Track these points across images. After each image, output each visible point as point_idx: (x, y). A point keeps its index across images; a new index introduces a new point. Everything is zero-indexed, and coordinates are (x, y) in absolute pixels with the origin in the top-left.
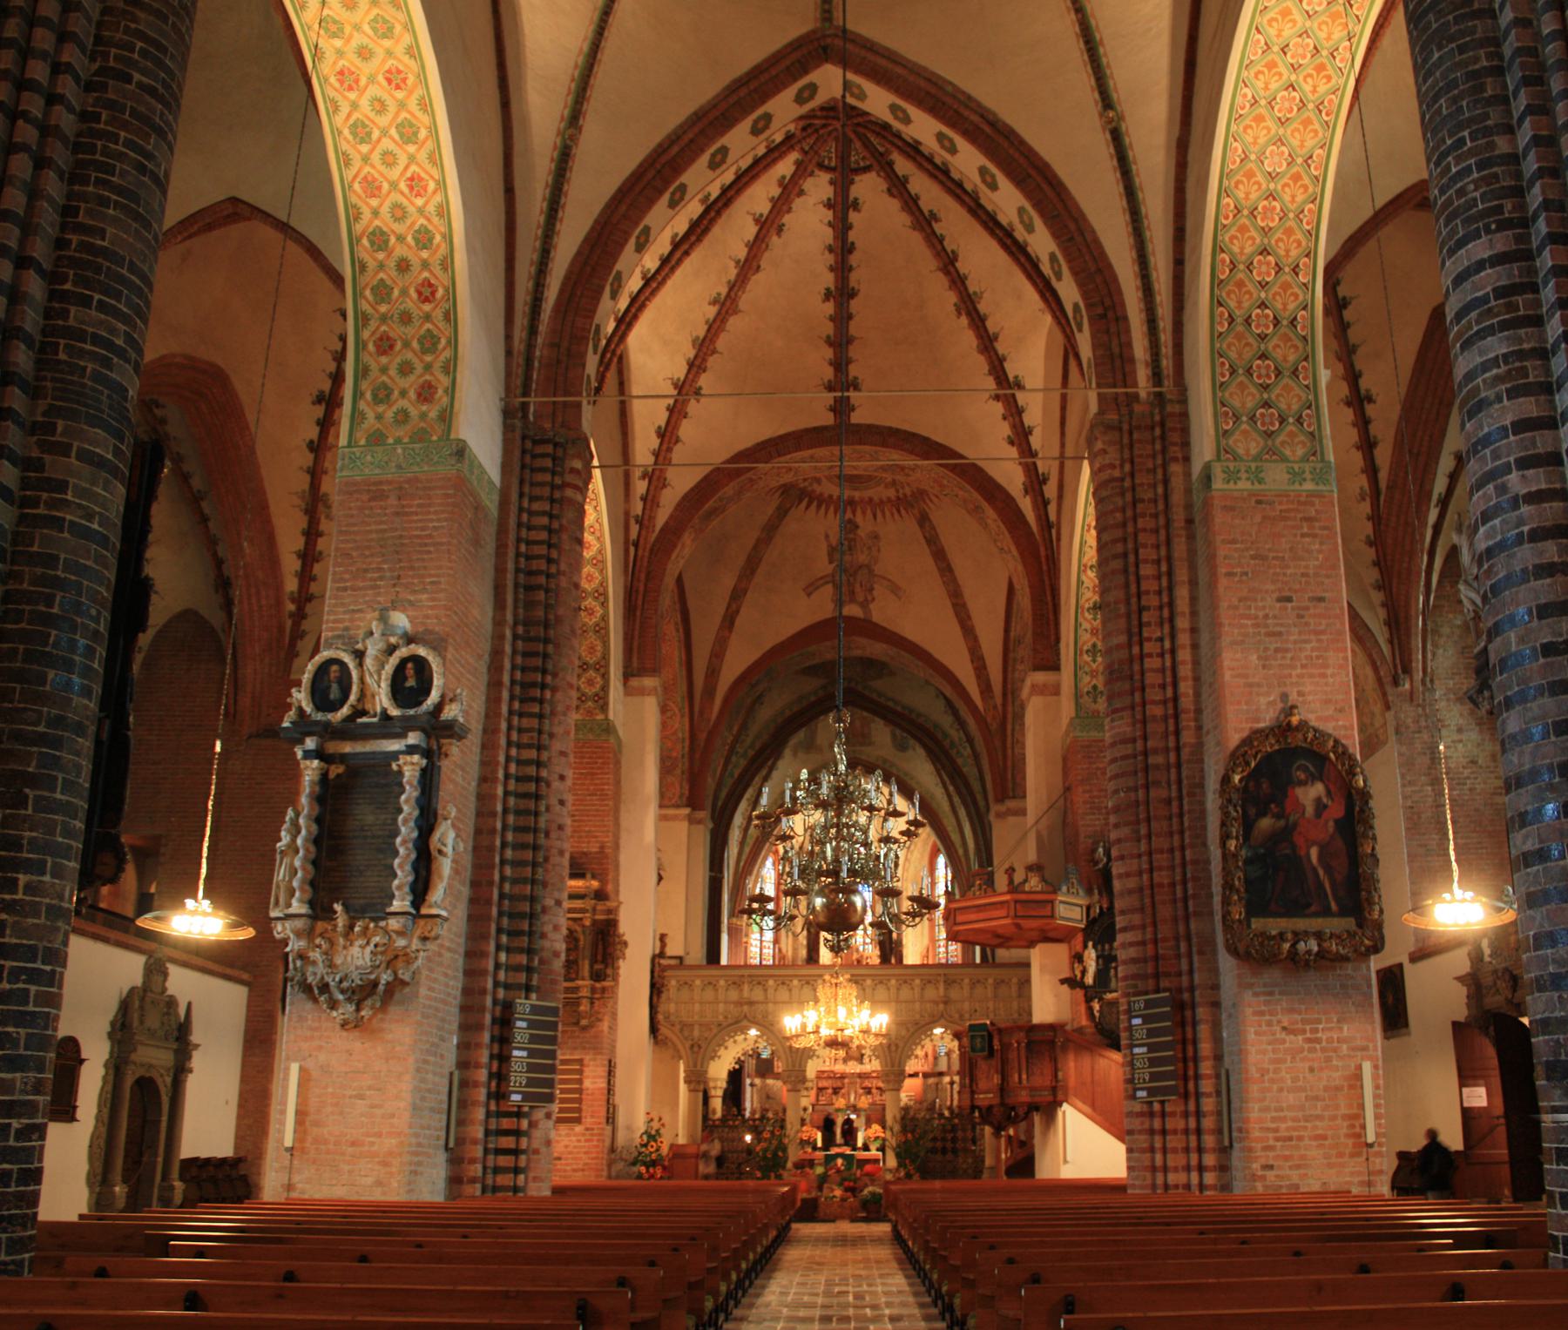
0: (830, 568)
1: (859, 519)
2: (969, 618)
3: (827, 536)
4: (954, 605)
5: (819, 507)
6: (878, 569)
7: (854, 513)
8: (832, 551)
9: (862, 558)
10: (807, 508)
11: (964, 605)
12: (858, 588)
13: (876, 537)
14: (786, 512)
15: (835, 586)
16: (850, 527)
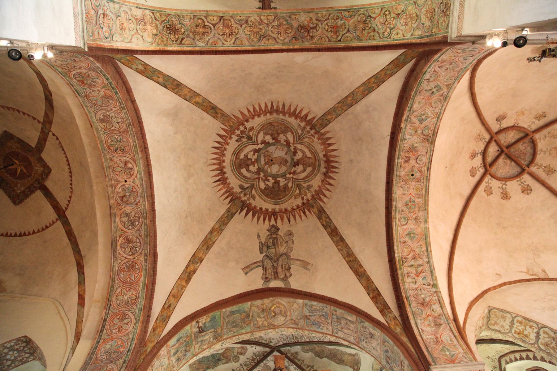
0: (260, 257)
1: (279, 224)
2: (361, 266)
3: (259, 236)
4: (348, 262)
5: (254, 215)
6: (293, 255)
7: (276, 220)
8: (263, 247)
9: (282, 249)
10: (246, 215)
11: (356, 259)
12: (280, 270)
13: (290, 234)
14: (233, 215)
15: (265, 269)
16: (274, 229)
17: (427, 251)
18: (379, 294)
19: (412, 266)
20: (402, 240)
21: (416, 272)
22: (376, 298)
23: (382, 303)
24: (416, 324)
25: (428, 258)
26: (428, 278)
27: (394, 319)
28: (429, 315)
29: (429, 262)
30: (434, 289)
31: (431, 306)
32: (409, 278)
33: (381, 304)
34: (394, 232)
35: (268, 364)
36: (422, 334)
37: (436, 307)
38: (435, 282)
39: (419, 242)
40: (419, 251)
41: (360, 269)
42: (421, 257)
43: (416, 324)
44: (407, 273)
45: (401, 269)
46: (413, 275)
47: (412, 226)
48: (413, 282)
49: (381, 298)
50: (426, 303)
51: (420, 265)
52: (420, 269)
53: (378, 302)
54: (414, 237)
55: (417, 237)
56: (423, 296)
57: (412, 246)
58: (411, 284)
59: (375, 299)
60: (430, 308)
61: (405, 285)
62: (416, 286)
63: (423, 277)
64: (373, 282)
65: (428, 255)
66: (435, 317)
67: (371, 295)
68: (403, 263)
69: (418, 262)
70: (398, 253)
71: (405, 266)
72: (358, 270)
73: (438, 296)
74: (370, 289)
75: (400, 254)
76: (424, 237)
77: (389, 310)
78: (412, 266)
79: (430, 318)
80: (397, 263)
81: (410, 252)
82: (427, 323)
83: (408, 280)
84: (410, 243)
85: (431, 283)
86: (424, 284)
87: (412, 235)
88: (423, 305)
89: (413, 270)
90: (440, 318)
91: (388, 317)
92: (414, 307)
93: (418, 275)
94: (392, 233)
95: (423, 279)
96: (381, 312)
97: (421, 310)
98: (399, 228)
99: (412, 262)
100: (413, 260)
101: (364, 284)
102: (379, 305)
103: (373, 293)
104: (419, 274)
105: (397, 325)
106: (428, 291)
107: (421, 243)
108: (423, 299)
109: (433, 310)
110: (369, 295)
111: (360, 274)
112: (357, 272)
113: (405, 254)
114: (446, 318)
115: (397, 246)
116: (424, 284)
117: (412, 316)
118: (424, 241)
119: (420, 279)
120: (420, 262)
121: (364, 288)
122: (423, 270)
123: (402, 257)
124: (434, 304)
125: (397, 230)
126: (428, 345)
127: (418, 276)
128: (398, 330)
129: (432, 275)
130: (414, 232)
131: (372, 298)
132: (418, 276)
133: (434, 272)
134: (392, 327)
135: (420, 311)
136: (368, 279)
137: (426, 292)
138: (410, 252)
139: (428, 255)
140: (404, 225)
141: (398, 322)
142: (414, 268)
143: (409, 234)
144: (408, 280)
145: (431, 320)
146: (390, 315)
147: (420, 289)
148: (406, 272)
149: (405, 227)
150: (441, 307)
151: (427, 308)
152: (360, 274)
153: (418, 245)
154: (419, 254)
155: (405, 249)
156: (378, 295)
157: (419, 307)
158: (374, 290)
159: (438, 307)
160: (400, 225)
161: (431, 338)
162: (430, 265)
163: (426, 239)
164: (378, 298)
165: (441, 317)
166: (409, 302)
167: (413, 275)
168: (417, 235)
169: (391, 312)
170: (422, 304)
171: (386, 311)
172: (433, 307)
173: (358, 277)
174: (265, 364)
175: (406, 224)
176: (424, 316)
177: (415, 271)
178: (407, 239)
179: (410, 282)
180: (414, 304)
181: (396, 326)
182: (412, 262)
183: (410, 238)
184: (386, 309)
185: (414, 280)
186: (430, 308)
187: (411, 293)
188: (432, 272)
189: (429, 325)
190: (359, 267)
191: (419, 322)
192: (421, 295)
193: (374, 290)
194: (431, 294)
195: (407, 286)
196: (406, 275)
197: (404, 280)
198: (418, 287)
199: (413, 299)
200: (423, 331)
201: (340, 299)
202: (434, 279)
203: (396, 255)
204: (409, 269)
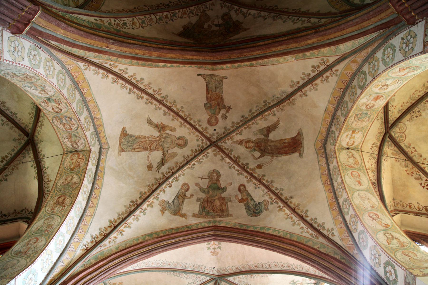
35: (207, 13)
174: (204, 10)
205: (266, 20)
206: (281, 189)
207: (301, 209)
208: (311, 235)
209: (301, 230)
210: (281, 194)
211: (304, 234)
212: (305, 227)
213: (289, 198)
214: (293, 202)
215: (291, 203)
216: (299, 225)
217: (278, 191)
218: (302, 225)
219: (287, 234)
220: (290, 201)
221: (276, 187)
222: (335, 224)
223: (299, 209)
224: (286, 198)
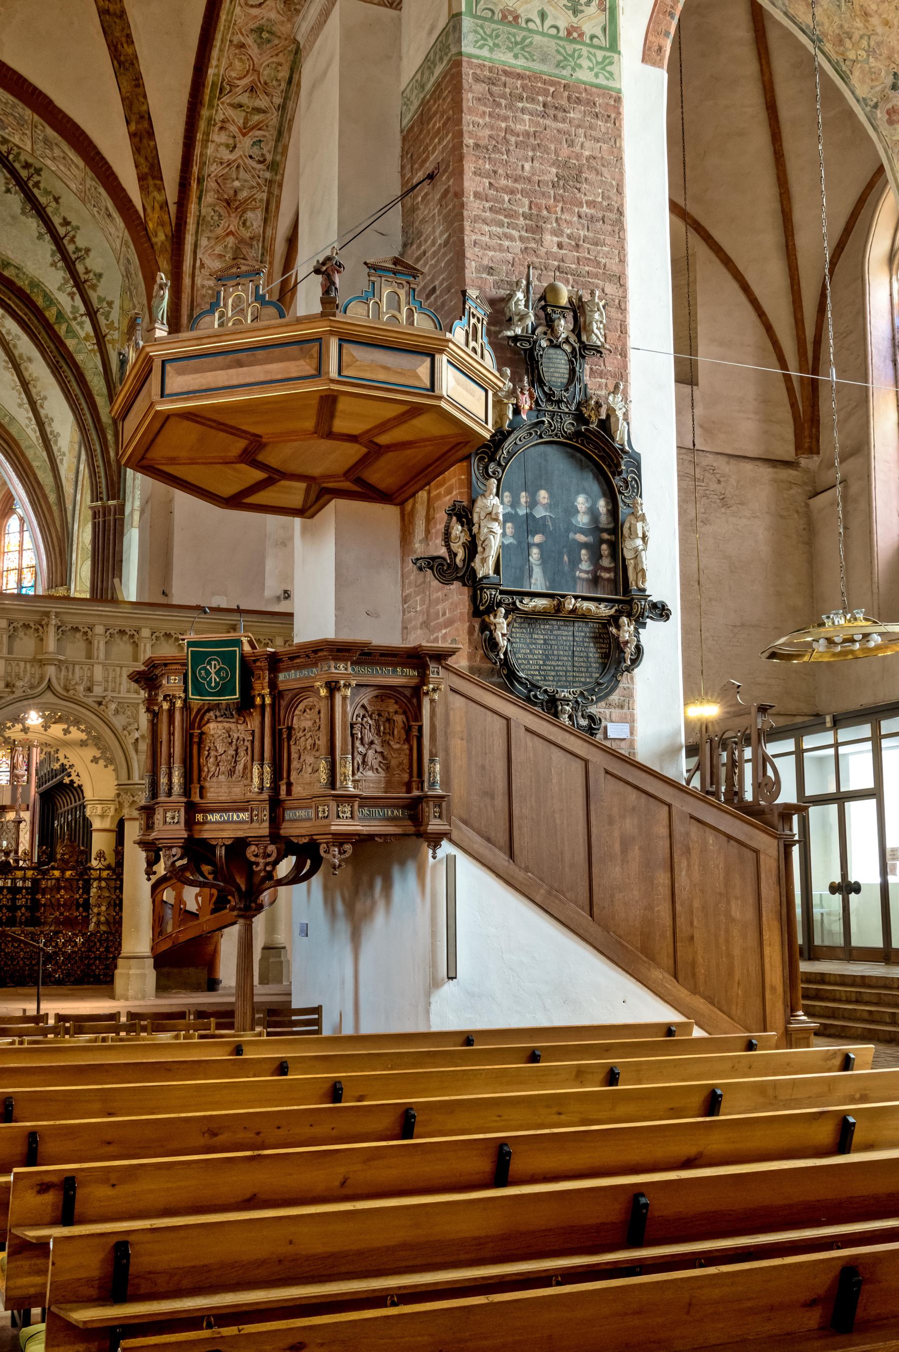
17: (290, 82)
18: (151, 134)
19: (241, 106)
20: (236, 40)
21: (245, 123)
22: (141, 140)
23: (150, 159)
24: (196, 246)
25: (286, 99)
26: (267, 144)
27: (161, 207)
28: (231, 233)
29: (283, 108)
30: (268, 175)
31: (244, 212)
32: (223, 134)
33: (146, 159)
34: (223, 17)
36: (197, 272)
37: (255, 218)
38: (278, 158)
39: (277, 55)
40: (269, 75)
41: (125, 45)
42: (270, 90)
43: (196, 246)
44: (223, 121)
45: (211, 106)
46: (233, 128)
47: (273, 15)
48: (227, 146)
49: (152, 143)
50: (237, 203)
51: (258, 110)
52: (257, 118)
53: (143, 152)
54: (269, 41)
55: (276, 41)
56: (237, 184)
57: (255, 60)
58: (222, 148)
59: (138, 139)
60: (240, 218)
61: (206, 147)
62: (232, 157)
63: (255, 139)
64: (145, 97)
65: (287, 91)
66: (242, 241)
67: (133, 127)
68: (221, 92)
69: (258, 100)
70: (217, 66)
71: (223, 103)
72: (119, 46)
73: (270, 193)
74: (135, 110)
75: (222, 72)
76: (293, 47)
77: (158, 182)
78: (241, 106)
79: (231, 240)
80: (207, 91)
81: (248, 72)
82: (218, 250)
83: (219, 138)
84: (254, 51)
85: (269, 157)
86: (251, 157)
87: (265, 35)
88: (229, 204)
89: (238, 117)
90: (251, 246)
91: (151, 197)
92: (210, 205)
93: (245, 130)
94: (218, 16)
95: (254, 144)
96: (141, 178)
97: (220, 216)
98: (238, 9)
99: (244, 99)
100: (247, 94)
101: (123, 90)
102: (142, 161)
103: (138, 123)
104: (249, 132)
105: (162, 224)
106: (253, 177)
107: (281, 58)
108: (235, 192)
109: (244, 223)
110: (128, 123)
111: (122, 58)
112: (116, 49)
113: (234, 75)
114: (263, 247)
115: (221, 50)
116: (251, 157)
117: (195, 226)
118: (291, 57)
119: (246, 143)
120: (262, 102)
121: (123, 100)
122: (262, 122)
123: (223, 80)
124: (253, 209)
125: (231, 13)
126: (198, 300)
127: (244, 135)
128: (160, 238)
129: (278, 140)
130: (274, 29)
131: (132, 135)
132: (244, 135)
133: (286, 134)
134: (151, 225)
135: (216, 218)
136: (138, 81)
137: (247, 177)
138: (248, 72)
139: (287, 91)
140: (252, 6)
141: (167, 217)
142: (244, 114)
143: (260, 30)
144: (219, 138)
145: (230, 245)
146: (156, 194)
147: (238, 167)
148: (220, 116)
149: (254, 11)
150: (265, 221)
151: (233, 215)
152: (122, 58)
153: (273, 63)
154: (266, 83)
155: (237, 63)
156: (148, 133)
157: (217, 208)
158: (142, 117)
159: (259, 218)
160: (243, 4)
161: (210, 288)
162: (282, 116)
163: (296, 53)
164: (145, 141)
165: (255, 243)
166: (202, 192)
167: (233, 128)
168: (279, 37)
169: (161, 189)
170: (228, 203)
171: (151, 182)
172: (249, 215)
173: (115, 63)
175: (260, 5)
176: (219, 231)
177: (241, 121)
178: (249, 41)
179: (222, 144)
180: (210, 198)
181: (160, 227)
182: (244, 99)
183: (259, 41)
184: (153, 178)
185: (231, 141)
186: (240, 218)
187: (214, 169)
188: (280, 133)
189: (220, 256)
190: (124, 39)
191: (204, 242)
192: (233, 181)
193: (142, 117)
194: (258, 184)
195: (209, 151)
196: (219, 125)
197: (208, 134)
198: (235, 161)
199: (213, 185)
200: (202, 265)
201: (61, 101)
202: (280, 150)
203: (211, 71)
204: (231, 113)
205: (9, 195)
206: (16, 335)
207: (39, 388)
208: (37, 437)
209: (27, 421)
210: (15, 346)
211: (29, 431)
212: (34, 421)
213: (25, 358)
214: (30, 371)
215: (26, 369)
216: (27, 411)
217: (10, 338)
218: (31, 415)
219: (6, 415)
220: (25, 364)
221: (8, 327)
222: (70, 452)
223: (35, 387)
224: (21, 356)
